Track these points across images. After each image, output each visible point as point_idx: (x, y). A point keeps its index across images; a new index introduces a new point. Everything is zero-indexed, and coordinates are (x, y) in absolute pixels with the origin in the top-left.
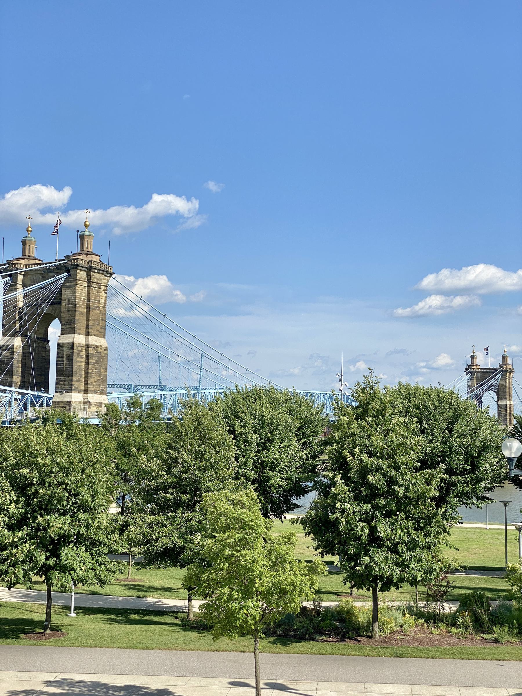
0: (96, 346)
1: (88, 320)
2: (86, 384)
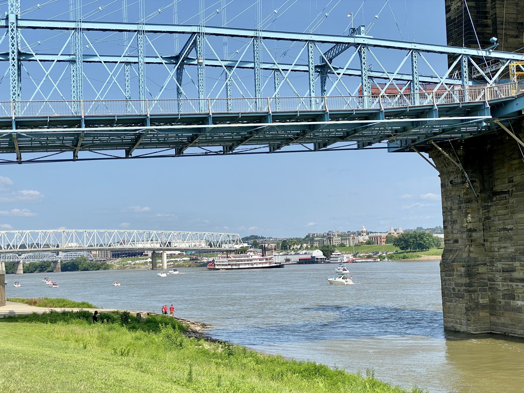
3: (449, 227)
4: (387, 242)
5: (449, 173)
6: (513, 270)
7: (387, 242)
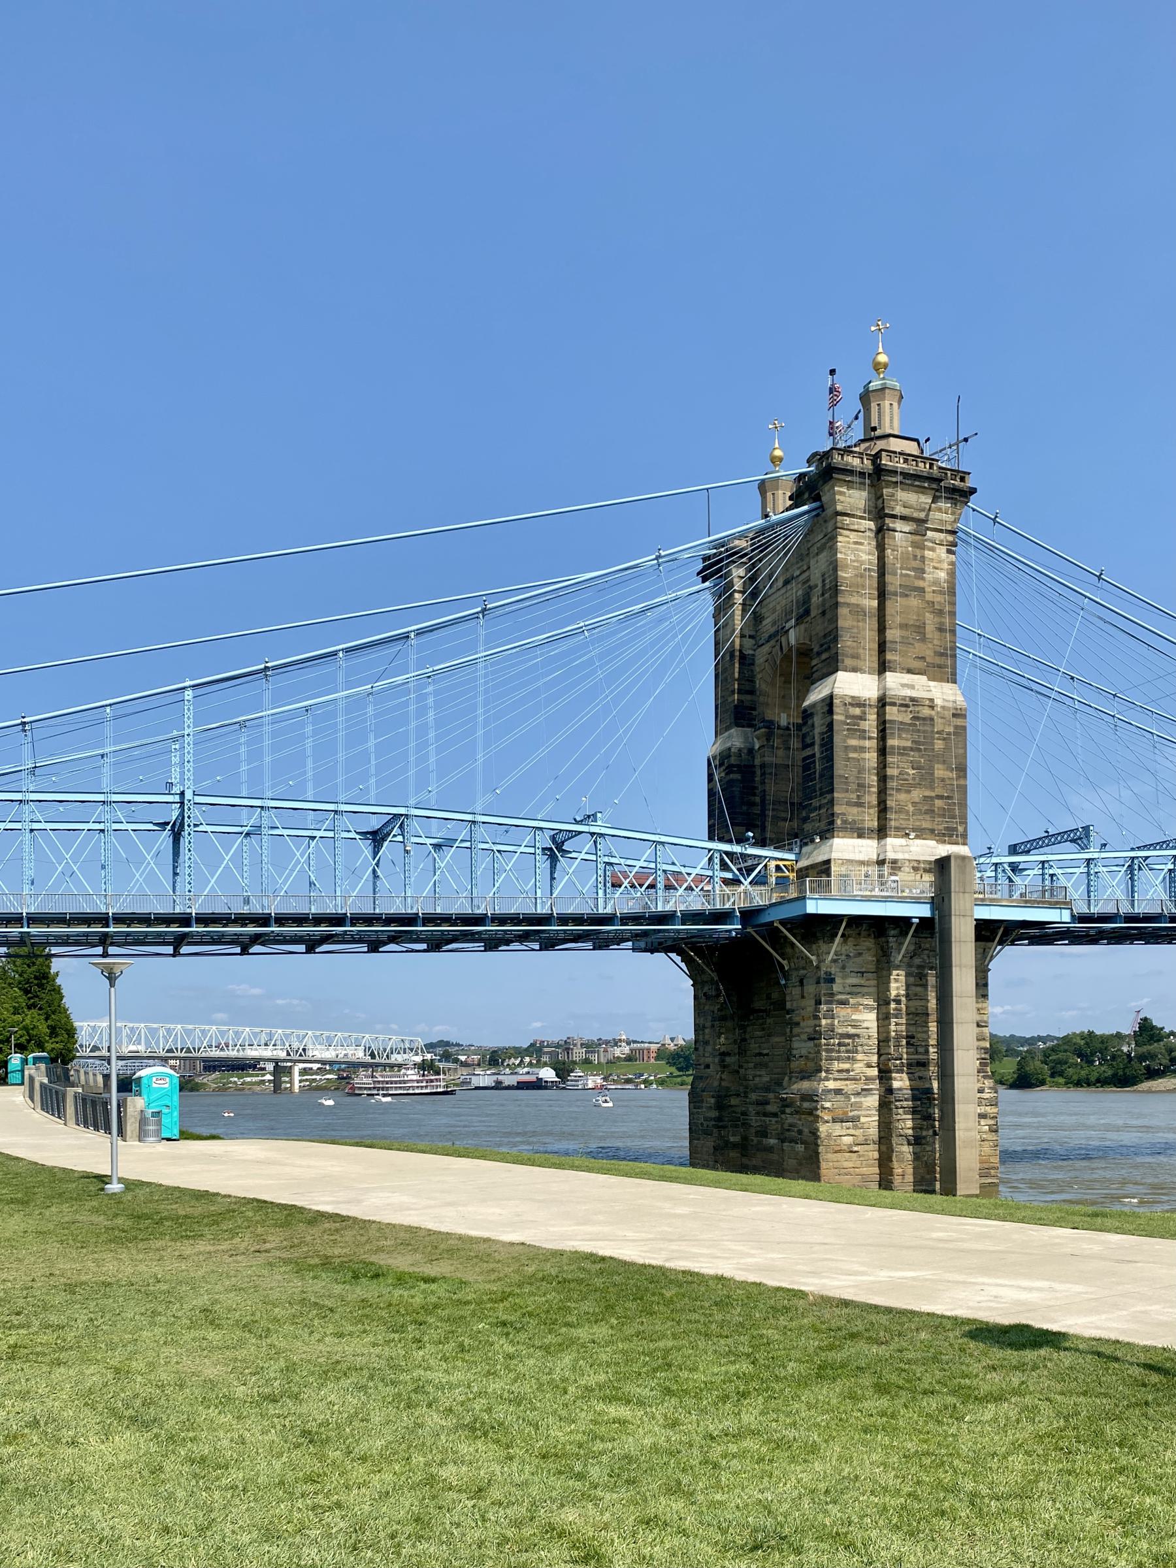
0: (912, 699)
1: (882, 629)
2: (883, 809)
3: (701, 1049)
4: (657, 1059)
5: (703, 983)
6: (767, 1103)
7: (657, 1059)
